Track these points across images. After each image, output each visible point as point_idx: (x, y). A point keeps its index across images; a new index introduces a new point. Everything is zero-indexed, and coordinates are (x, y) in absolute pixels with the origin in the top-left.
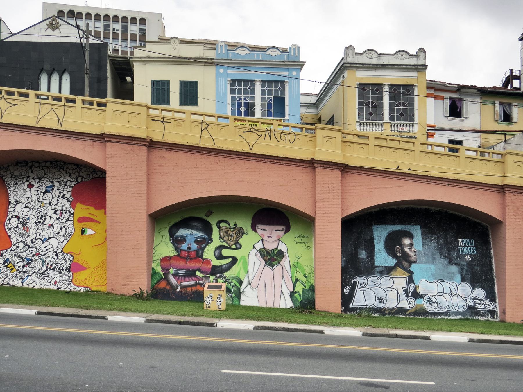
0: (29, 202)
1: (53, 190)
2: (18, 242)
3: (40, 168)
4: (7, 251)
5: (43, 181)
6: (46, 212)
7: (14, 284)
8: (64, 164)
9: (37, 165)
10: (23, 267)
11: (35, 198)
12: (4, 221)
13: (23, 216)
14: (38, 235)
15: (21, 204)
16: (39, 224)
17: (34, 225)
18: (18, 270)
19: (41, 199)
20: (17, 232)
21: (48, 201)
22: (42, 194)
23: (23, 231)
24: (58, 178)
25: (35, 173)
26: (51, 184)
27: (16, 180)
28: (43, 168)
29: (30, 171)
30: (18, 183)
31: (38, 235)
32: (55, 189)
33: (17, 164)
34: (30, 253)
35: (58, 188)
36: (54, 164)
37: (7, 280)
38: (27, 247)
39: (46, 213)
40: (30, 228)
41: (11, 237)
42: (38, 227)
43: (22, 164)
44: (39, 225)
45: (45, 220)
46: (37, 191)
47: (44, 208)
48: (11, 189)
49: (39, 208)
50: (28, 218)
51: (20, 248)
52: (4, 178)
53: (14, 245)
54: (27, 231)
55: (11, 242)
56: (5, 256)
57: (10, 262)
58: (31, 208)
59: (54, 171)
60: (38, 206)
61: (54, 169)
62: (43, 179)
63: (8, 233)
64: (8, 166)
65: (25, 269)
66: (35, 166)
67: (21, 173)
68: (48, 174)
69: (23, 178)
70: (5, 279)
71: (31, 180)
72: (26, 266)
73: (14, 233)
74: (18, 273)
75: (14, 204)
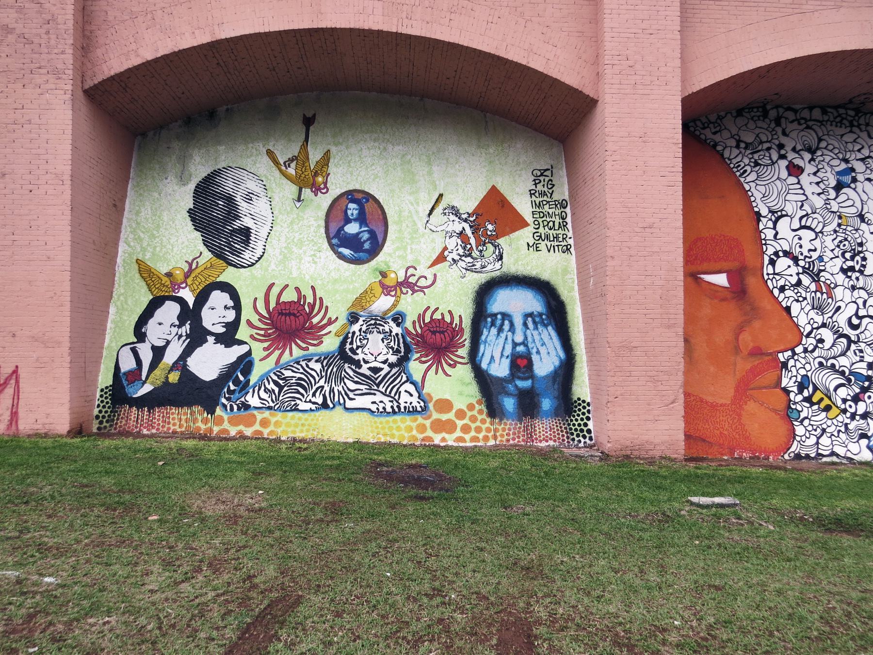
0: (807, 215)
1: (854, 180)
2: (815, 325)
3: (800, 124)
4: (794, 354)
5: (821, 158)
6: (859, 241)
7: (849, 455)
8: (856, 115)
9: (791, 115)
10: (856, 399)
11: (819, 202)
12: (759, 265)
13: (806, 253)
14: (861, 306)
15: (787, 219)
16: (855, 275)
17: (840, 278)
18: (844, 411)
19: (834, 206)
20: (805, 299)
21: (853, 210)
22: (833, 194)
23: (819, 294)
24: (856, 148)
25: (794, 134)
26: (843, 166)
27: (752, 153)
28: (810, 123)
29: (779, 130)
30: (760, 162)
31: (861, 306)
32: (860, 177)
33: (740, 113)
34: (858, 359)
35: (867, 176)
36: (832, 113)
37: (825, 440)
38: (844, 340)
39: (861, 244)
40: (832, 286)
41: (794, 313)
42: (851, 283)
43: (752, 114)
44: (853, 278)
45: (864, 263)
46: (818, 183)
47: (849, 228)
48: (749, 179)
49: (837, 229)
50: (820, 258)
51: (828, 344)
52: (719, 148)
53: (808, 336)
54: (830, 296)
55: (797, 326)
56: (793, 369)
57: (816, 388)
58: (818, 230)
59: (842, 131)
60: (834, 225)
61: (836, 126)
62: (819, 153)
63: (780, 299)
64: (720, 118)
65: (861, 408)
66: (786, 118)
67: (757, 136)
68: (825, 137)
69: (769, 149)
70: (818, 438)
71: (791, 156)
72: (861, 396)
73: (798, 301)
74: (848, 421)
75: (771, 220)
